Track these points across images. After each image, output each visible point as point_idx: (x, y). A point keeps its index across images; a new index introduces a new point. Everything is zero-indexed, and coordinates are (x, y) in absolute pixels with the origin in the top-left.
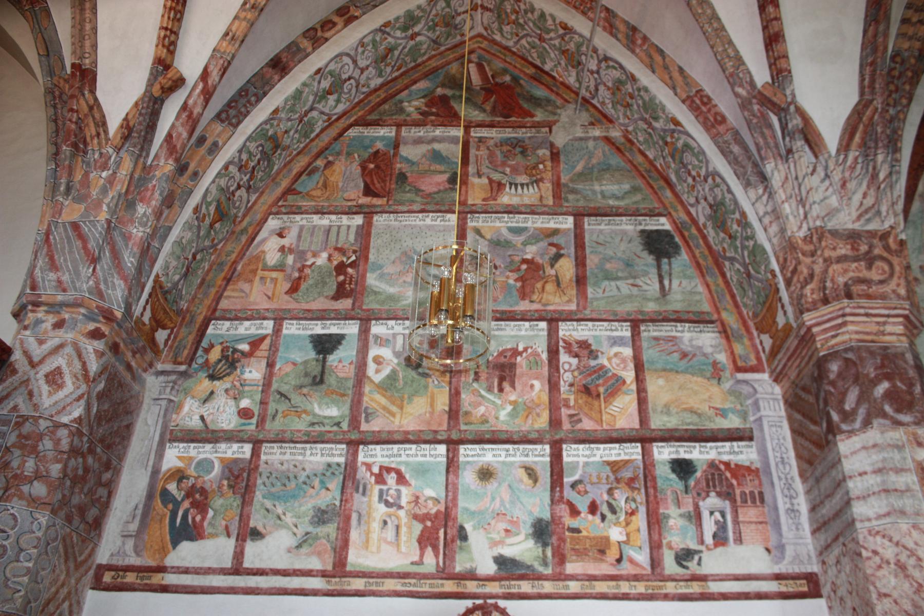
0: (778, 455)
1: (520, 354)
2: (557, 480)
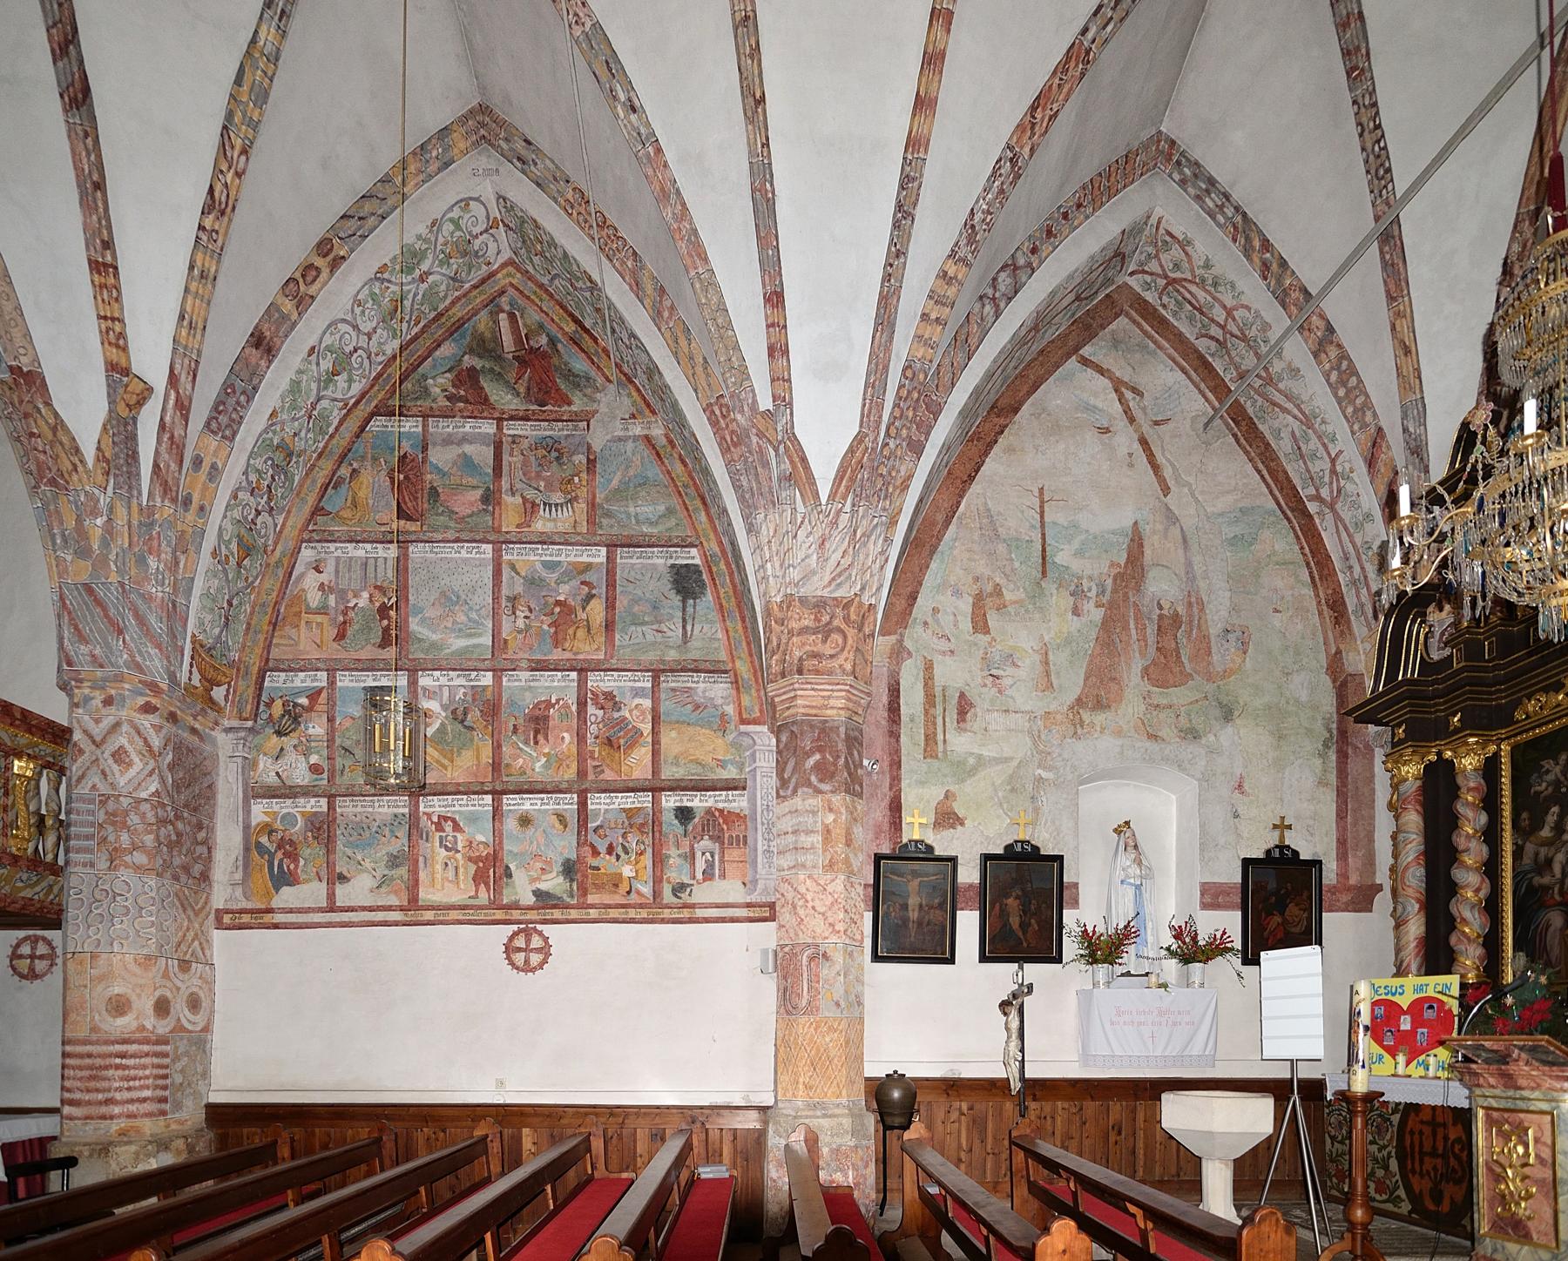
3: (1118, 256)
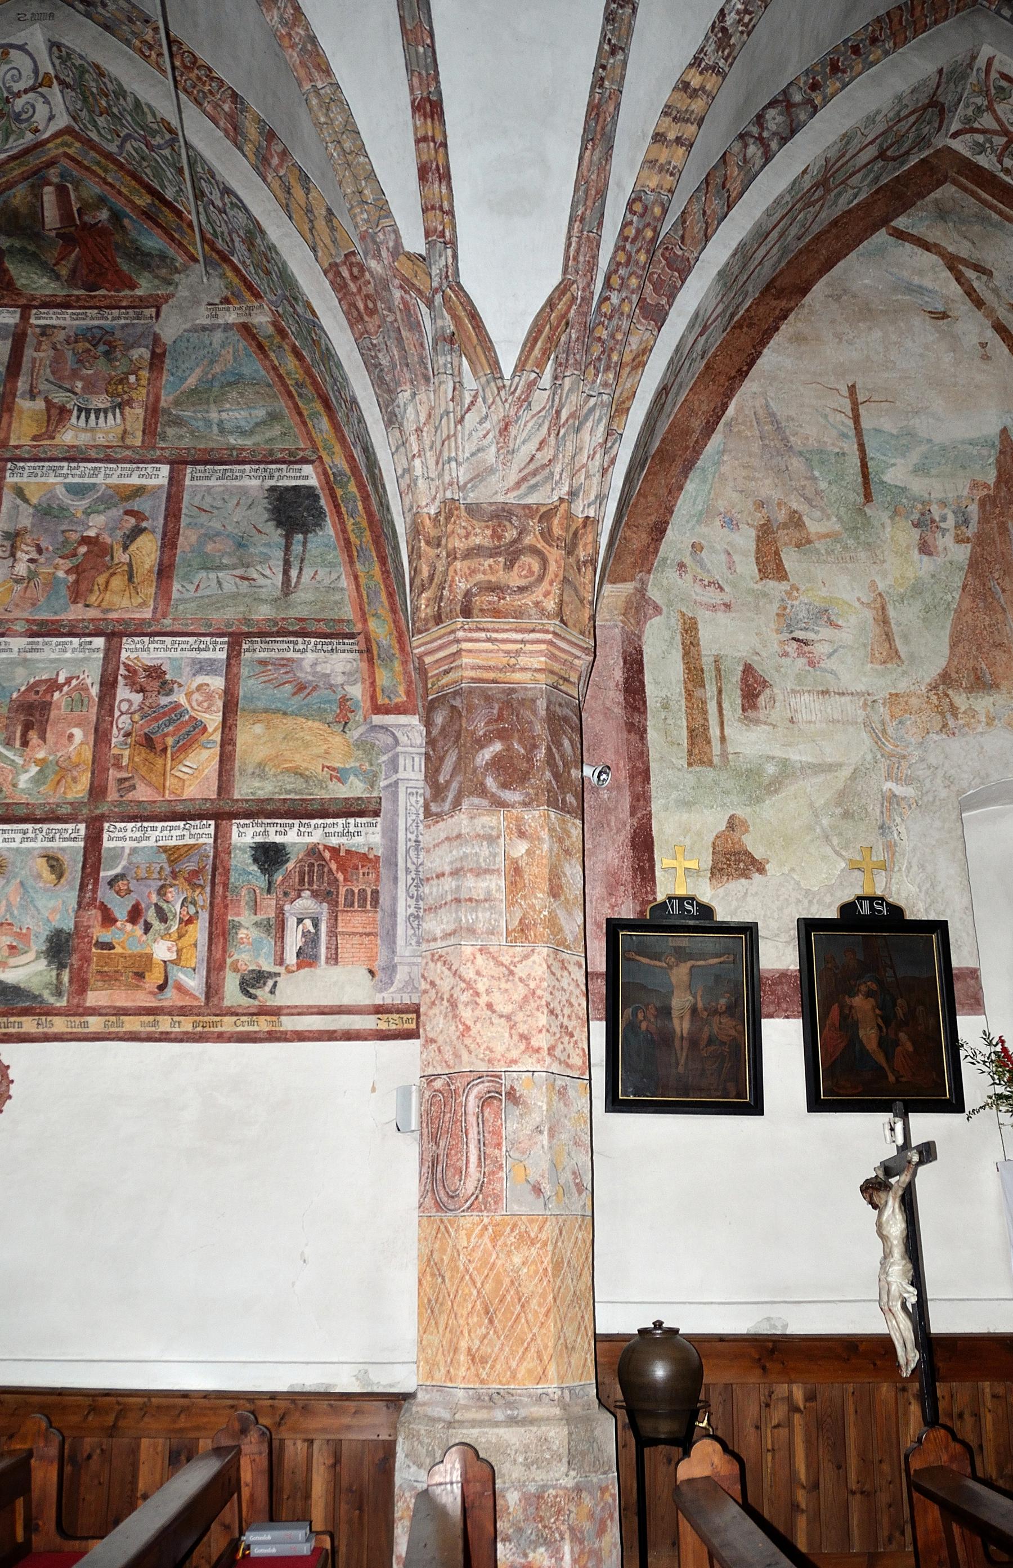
0: (413, 837)
1: (60, 688)
2: (90, 874)
3: (933, 107)
